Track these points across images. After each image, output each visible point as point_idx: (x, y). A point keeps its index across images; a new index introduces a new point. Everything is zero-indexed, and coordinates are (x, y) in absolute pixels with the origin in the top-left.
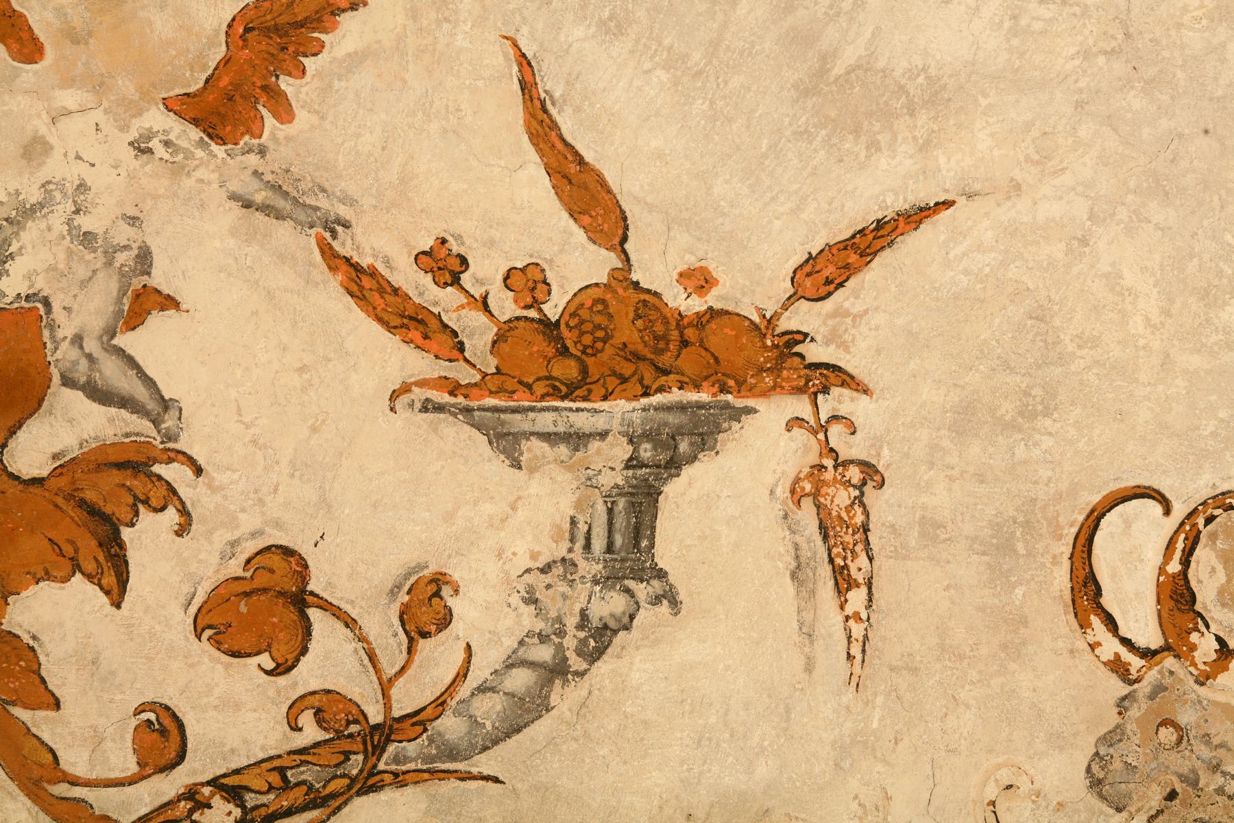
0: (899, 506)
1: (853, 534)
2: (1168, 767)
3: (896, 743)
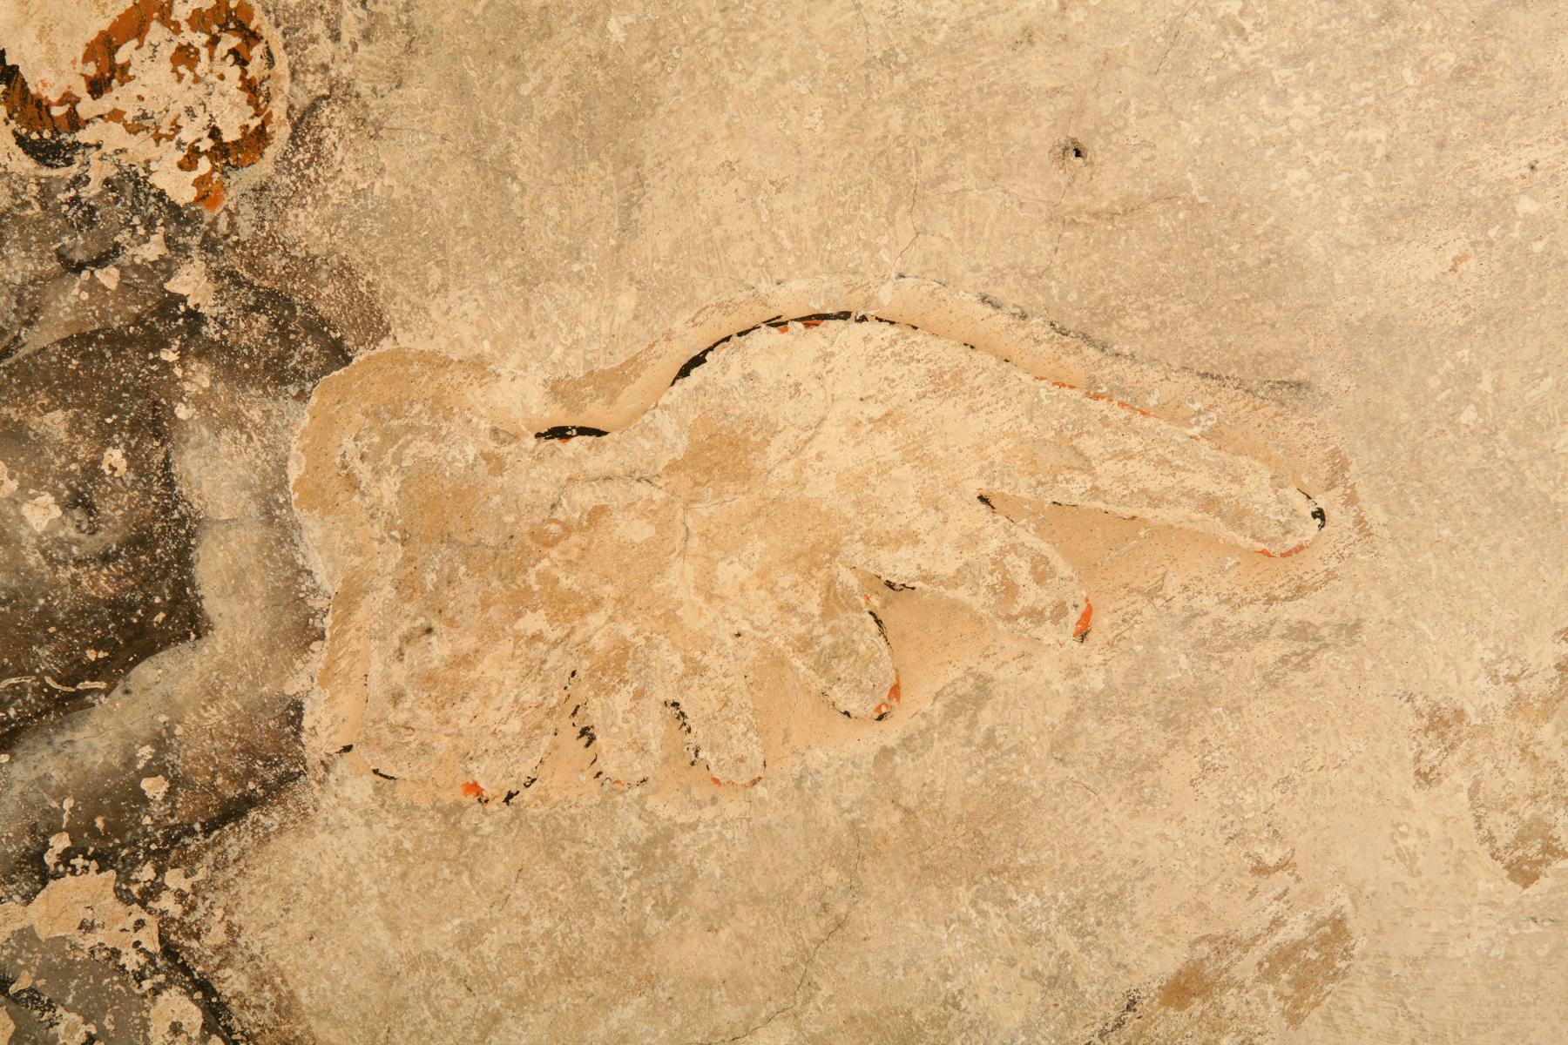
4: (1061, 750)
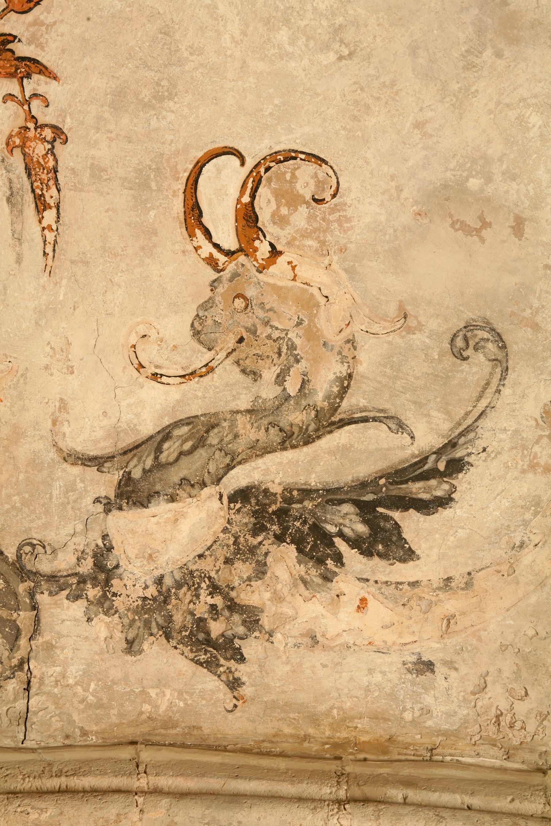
0: (77, 156)
1: (47, 174)
2: (239, 323)
3: (74, 309)
4: (13, 414)
